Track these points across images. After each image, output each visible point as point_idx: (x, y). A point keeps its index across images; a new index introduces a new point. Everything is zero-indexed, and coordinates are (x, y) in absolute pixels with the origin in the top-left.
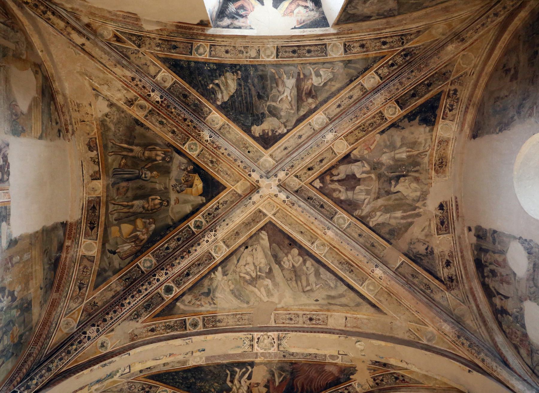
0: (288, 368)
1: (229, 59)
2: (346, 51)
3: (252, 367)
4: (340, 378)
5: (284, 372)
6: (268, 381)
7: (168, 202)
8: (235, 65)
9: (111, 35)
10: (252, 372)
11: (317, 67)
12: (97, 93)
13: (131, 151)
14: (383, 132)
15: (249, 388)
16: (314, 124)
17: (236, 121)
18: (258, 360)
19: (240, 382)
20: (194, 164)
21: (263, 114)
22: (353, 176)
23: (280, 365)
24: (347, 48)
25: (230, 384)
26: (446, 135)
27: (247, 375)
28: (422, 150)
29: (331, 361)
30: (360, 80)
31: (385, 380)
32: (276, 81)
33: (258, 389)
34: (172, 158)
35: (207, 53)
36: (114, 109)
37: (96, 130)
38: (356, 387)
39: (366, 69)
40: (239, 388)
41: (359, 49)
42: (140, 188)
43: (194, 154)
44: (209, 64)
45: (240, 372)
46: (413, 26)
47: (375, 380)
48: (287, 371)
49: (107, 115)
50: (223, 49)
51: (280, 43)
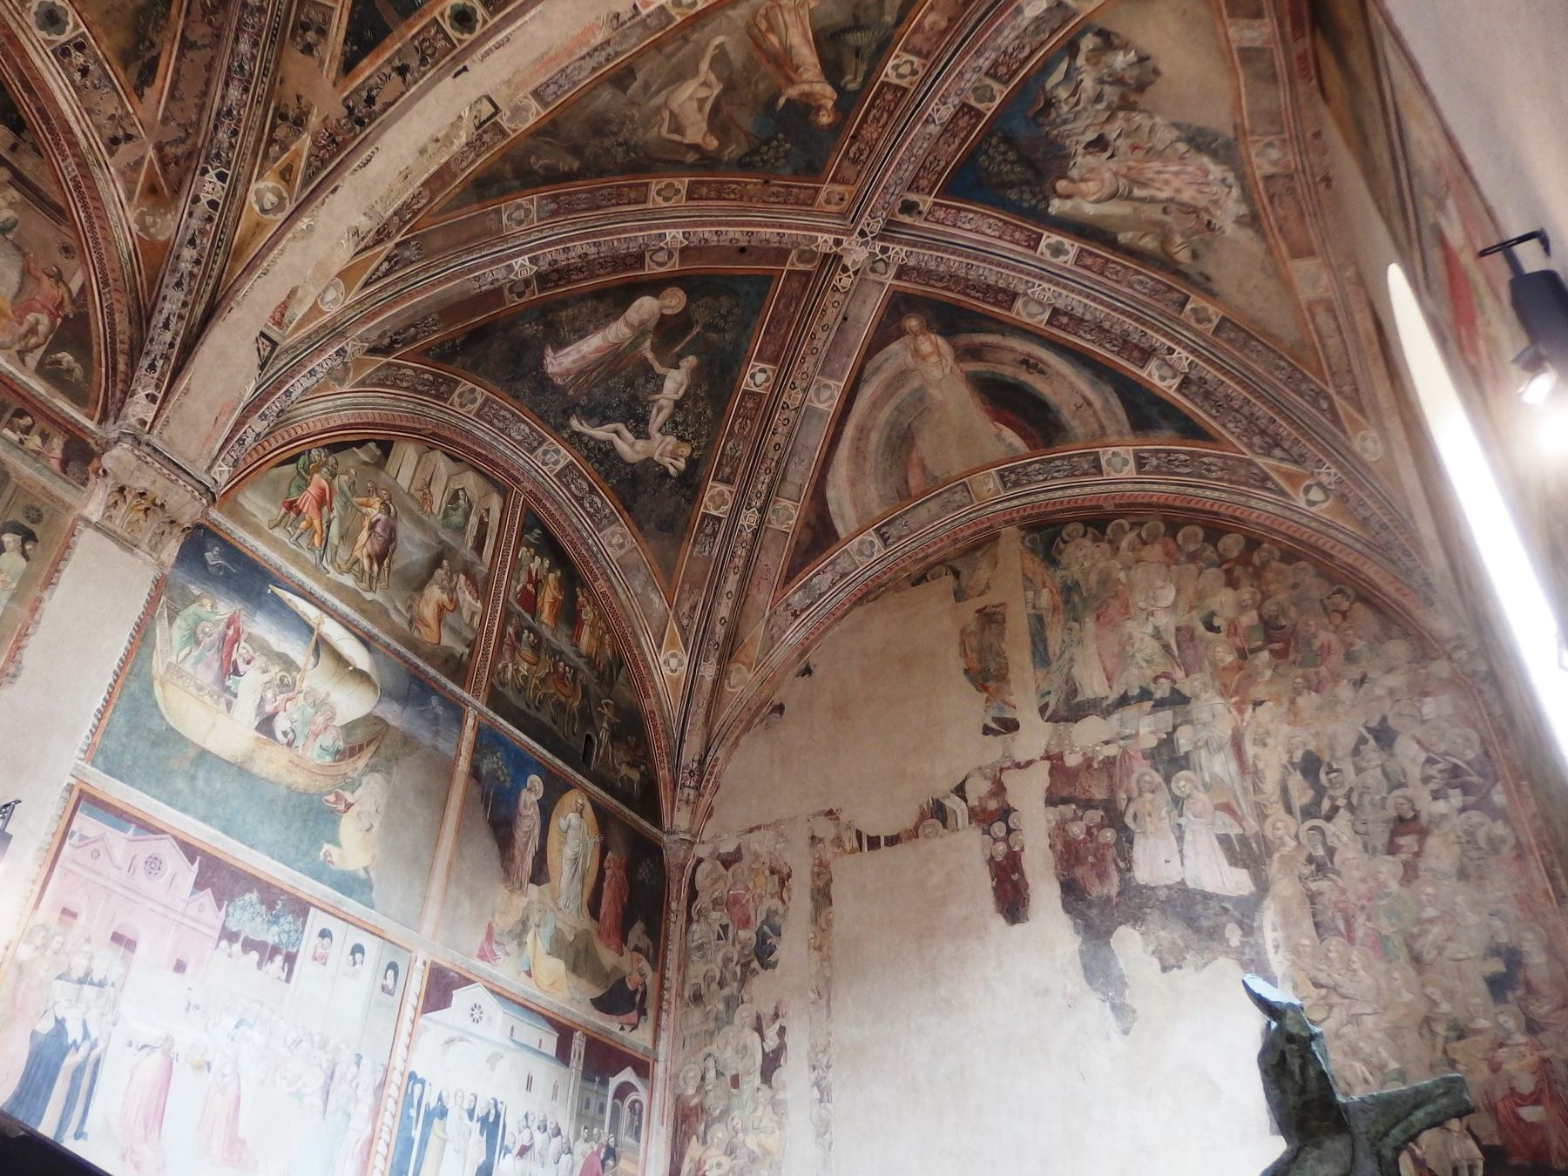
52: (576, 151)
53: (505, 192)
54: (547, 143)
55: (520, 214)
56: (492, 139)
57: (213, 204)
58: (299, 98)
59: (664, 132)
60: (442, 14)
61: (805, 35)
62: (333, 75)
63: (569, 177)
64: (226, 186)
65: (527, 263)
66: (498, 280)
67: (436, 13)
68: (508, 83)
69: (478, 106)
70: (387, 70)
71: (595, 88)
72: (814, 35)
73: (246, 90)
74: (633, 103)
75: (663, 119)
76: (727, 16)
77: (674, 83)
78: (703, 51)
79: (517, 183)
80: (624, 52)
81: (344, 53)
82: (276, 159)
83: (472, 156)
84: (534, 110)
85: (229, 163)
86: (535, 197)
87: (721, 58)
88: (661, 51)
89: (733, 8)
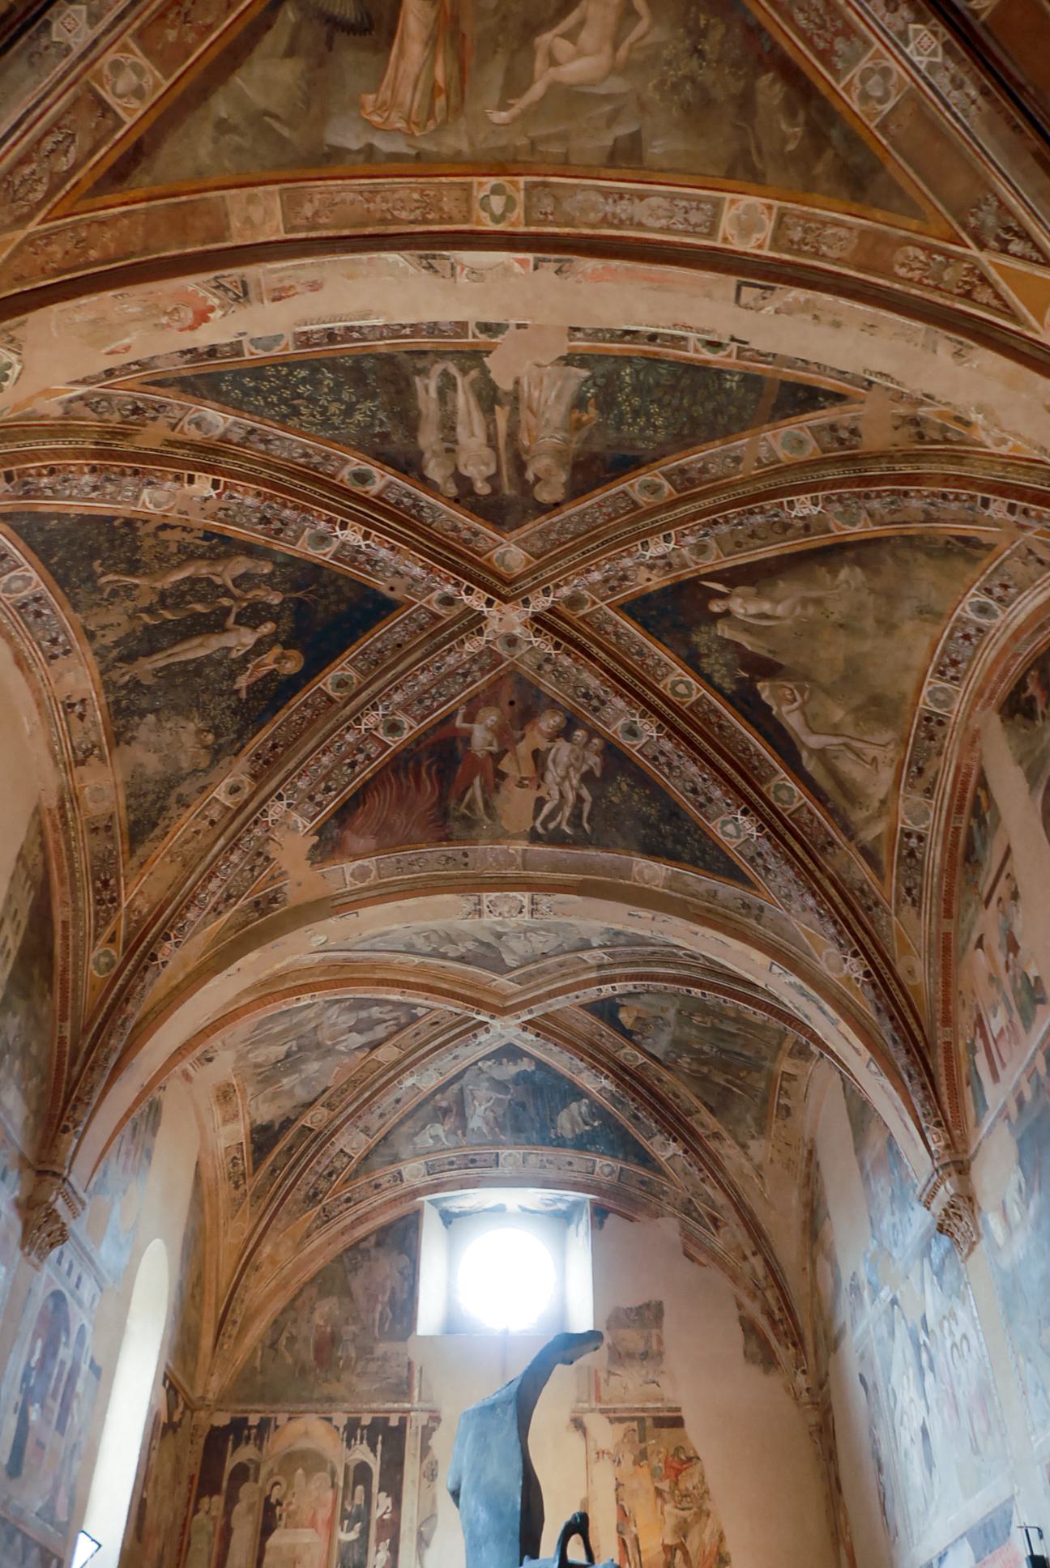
0: (455, 827)
1: (568, 1154)
2: (400, 1173)
3: (533, 829)
4: (339, 827)
5: (464, 817)
6: (497, 788)
7: (679, 1012)
8: (558, 1146)
9: (722, 1231)
10: (535, 818)
11: (439, 1147)
12: (758, 1169)
13: (728, 1081)
14: (324, 1092)
15: (542, 777)
16: (435, 1075)
17: (560, 1077)
18: (521, 846)
19: (562, 795)
20: (631, 1040)
21: (517, 1084)
22: (360, 1032)
23: (474, 833)
24: (399, 1177)
25: (585, 793)
26: (230, 1127)
27: (546, 810)
28: (260, 1097)
29: (365, 862)
30: (372, 1142)
31: (247, 874)
32: (498, 1124)
33: (519, 770)
34: (667, 1053)
35: (598, 1165)
36: (741, 1140)
37: (774, 1126)
38: (299, 819)
39: (366, 1158)
40: (564, 778)
41: (381, 1181)
42: (723, 1041)
43: (629, 1050)
44: (597, 1152)
45: (560, 824)
46: (317, 1241)
47: (267, 859)
48: (456, 819)
49: (753, 1137)
50: (575, 1168)
51: (493, 1172)
52: (745, 102)
53: (853, 140)
54: (759, 151)
55: (875, 87)
56: (796, 225)
57: (1012, 509)
58: (896, 428)
59: (644, 24)
60: (729, 356)
61: (402, 53)
62: (856, 406)
63: (790, 72)
64: (991, 497)
65: (912, 46)
66: (953, 80)
67: (733, 360)
68: (709, 295)
69: (752, 304)
70: (815, 368)
71: (662, 170)
72: (390, 46)
73: (906, 494)
74: (643, 107)
75: (631, 49)
76: (472, 143)
77: (584, 94)
78: (524, 114)
79: (835, 134)
80: (598, 189)
81: (833, 405)
82: (960, 433)
83: (829, 231)
84: (733, 211)
85: (972, 498)
86: (839, 88)
87: (515, 85)
88: (566, 155)
89: (459, 153)
